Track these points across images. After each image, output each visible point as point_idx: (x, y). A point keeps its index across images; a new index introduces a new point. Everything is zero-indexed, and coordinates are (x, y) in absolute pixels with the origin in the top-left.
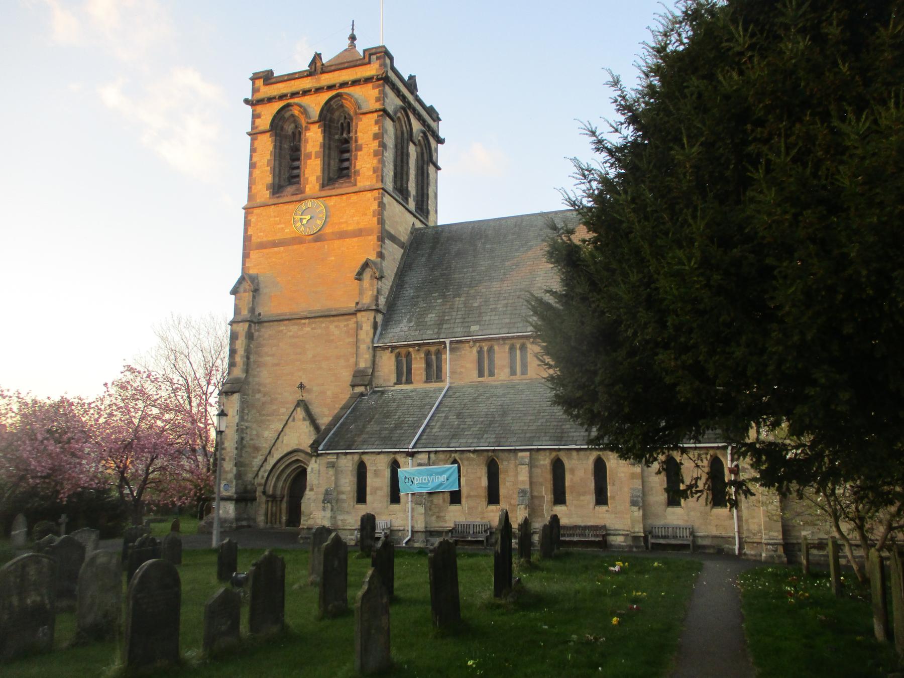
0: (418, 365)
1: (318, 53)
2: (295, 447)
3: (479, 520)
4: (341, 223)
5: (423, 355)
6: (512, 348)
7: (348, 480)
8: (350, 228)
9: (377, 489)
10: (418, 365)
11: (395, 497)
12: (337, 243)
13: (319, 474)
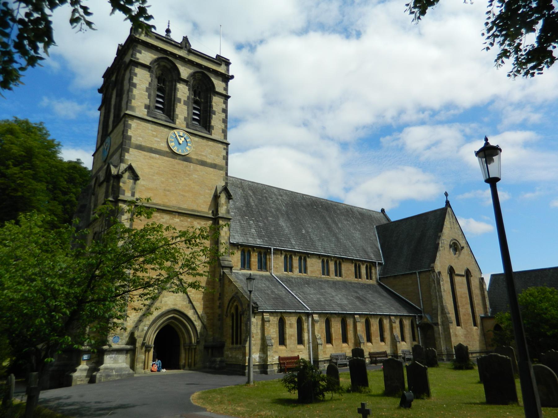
0: (254, 259)
1: (185, 36)
2: (172, 307)
3: (340, 352)
4: (203, 155)
5: (257, 254)
6: (300, 259)
7: (275, 330)
8: (209, 161)
9: (292, 336)
10: (254, 259)
11: (300, 341)
12: (199, 167)
13: (257, 325)
